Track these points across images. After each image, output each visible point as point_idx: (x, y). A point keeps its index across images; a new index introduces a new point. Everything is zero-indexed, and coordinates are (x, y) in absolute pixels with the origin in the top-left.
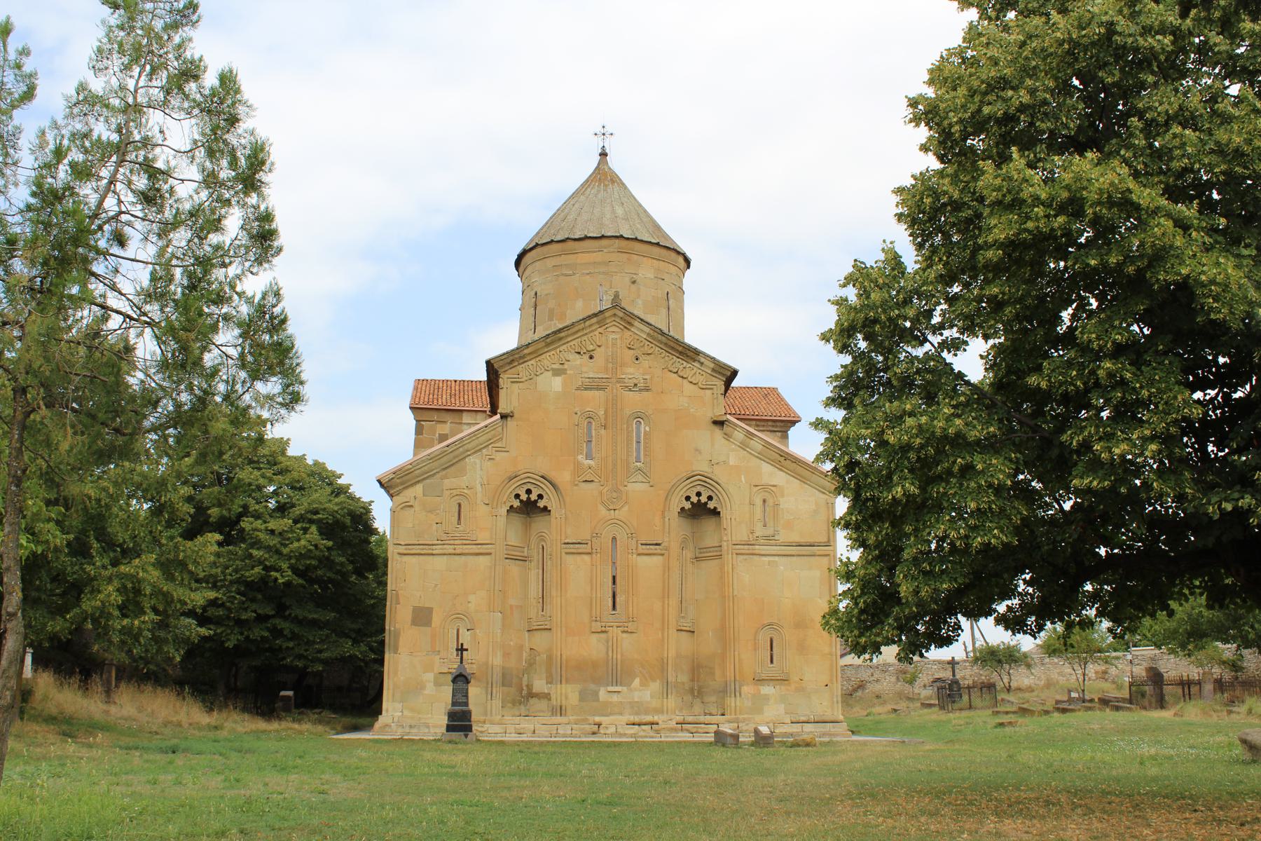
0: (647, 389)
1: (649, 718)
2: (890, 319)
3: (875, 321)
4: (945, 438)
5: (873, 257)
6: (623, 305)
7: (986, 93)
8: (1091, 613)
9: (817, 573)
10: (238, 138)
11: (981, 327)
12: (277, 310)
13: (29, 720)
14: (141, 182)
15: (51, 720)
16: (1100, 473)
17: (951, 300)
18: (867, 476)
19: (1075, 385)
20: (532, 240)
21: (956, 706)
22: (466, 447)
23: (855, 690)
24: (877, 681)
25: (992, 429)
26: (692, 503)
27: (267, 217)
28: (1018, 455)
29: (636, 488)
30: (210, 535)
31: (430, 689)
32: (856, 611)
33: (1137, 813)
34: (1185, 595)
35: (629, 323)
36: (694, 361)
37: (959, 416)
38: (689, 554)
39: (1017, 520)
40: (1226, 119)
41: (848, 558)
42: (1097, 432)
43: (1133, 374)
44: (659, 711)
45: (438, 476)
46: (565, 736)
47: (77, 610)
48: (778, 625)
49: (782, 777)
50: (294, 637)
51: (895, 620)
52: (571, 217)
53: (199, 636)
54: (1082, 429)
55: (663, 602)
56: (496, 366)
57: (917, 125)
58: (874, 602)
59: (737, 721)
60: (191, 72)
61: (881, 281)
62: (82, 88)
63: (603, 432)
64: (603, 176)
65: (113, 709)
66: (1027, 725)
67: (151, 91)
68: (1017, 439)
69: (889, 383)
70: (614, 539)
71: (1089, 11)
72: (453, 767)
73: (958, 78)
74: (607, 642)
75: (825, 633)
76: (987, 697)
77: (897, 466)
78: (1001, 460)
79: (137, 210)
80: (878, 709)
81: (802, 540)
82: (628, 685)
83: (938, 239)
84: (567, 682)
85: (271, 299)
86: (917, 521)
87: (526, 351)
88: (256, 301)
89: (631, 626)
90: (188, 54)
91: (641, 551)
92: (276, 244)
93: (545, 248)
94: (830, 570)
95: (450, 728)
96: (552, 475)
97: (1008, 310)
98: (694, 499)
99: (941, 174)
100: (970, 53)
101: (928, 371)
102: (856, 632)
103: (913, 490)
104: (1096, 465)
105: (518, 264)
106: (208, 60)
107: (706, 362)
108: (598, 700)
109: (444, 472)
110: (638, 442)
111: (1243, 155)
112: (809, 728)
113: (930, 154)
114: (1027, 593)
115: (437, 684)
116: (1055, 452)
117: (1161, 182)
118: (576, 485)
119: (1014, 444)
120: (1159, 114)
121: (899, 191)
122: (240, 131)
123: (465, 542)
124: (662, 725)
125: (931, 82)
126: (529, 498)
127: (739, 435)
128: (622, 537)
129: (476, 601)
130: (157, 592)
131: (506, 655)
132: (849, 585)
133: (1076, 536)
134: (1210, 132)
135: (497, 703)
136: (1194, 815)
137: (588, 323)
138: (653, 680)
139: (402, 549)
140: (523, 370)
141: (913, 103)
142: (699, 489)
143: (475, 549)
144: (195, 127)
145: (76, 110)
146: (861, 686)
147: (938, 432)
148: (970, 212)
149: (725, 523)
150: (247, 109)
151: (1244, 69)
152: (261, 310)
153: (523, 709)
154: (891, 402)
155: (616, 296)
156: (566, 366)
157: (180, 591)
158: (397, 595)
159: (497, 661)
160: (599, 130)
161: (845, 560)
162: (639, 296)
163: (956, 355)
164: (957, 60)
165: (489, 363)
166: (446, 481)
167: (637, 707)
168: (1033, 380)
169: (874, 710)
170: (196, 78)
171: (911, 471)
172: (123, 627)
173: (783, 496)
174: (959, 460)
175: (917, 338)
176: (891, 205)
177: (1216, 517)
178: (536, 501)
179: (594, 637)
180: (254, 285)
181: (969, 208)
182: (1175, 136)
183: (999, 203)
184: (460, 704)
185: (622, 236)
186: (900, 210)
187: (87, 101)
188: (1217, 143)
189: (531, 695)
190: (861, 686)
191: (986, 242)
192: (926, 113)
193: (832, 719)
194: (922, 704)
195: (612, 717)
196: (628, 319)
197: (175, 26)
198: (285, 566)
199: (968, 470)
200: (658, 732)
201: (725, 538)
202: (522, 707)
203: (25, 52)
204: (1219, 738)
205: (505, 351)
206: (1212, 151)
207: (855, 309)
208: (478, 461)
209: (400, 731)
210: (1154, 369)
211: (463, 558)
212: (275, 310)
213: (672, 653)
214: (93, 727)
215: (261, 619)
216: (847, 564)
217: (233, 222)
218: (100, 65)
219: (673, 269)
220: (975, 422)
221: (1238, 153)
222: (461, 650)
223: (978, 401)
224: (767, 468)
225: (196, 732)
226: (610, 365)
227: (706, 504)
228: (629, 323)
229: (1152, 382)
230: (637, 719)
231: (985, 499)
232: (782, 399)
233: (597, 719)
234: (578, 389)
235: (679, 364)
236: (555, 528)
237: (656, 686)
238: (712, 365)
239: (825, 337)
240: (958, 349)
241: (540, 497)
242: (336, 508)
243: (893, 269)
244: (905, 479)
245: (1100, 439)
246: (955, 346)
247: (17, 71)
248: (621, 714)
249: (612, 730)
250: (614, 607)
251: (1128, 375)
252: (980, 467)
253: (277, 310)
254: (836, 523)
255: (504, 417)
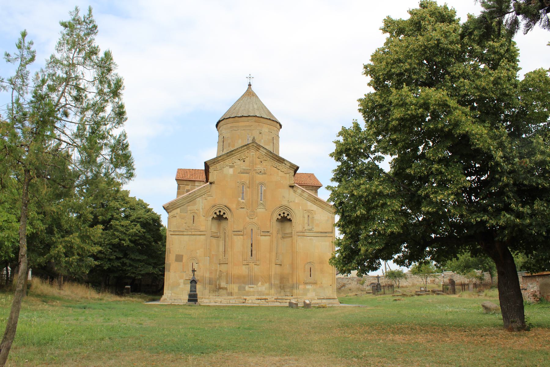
0: (265, 174)
1: (264, 297)
2: (355, 149)
3: (350, 149)
4: (375, 193)
5: (349, 126)
6: (256, 142)
7: (393, 64)
8: (428, 258)
9: (328, 243)
10: (111, 77)
11: (389, 150)
12: (125, 142)
13: (30, 296)
14: (74, 93)
15: (38, 296)
16: (432, 206)
17: (379, 142)
18: (346, 207)
19: (424, 173)
20: (222, 117)
21: (379, 293)
22: (196, 195)
23: (342, 287)
24: (350, 284)
25: (393, 190)
26: (281, 217)
27: (122, 107)
28: (403, 200)
29: (260, 210)
30: (99, 225)
31: (182, 286)
32: (342, 257)
33: (444, 332)
34: (463, 252)
35: (258, 149)
36: (283, 163)
37: (381, 185)
38: (280, 236)
39: (402, 224)
40: (479, 77)
41: (339, 238)
42: (432, 190)
43: (445, 170)
44: (268, 295)
45: (185, 205)
46: (232, 303)
47: (48, 254)
48: (313, 262)
49: (314, 319)
50: (130, 265)
51: (356, 261)
52: (237, 109)
53: (95, 265)
54: (426, 189)
55: (270, 254)
56: (208, 164)
57: (367, 75)
58: (349, 254)
59: (297, 298)
60: (94, 52)
61: (352, 134)
62: (52, 57)
63: (248, 189)
64: (249, 93)
65: (62, 292)
66: (405, 300)
67: (79, 58)
68: (402, 194)
69: (355, 173)
70: (252, 230)
71: (431, 35)
72: (190, 315)
73: (382, 59)
74: (249, 268)
75: (330, 266)
76: (391, 290)
77: (358, 204)
78: (397, 201)
79: (73, 103)
80: (350, 294)
81: (323, 231)
82: (257, 284)
83: (374, 119)
84: (234, 283)
85: (123, 138)
86: (366, 224)
87: (219, 159)
88: (117, 138)
89: (258, 263)
90: (93, 45)
91: (262, 234)
92: (125, 117)
93: (227, 120)
94: (332, 242)
95: (189, 300)
96: (229, 205)
97: (399, 144)
98: (282, 215)
99: (375, 94)
100: (386, 50)
101: (370, 169)
102: (342, 265)
103: (364, 212)
104: (431, 203)
105: (217, 126)
106: (100, 47)
107: (287, 164)
108: (245, 290)
109: (188, 204)
110: (261, 193)
111: (486, 89)
112: (324, 301)
113: (371, 87)
114: (405, 251)
115: (185, 284)
116: (416, 199)
117: (456, 99)
119: (401, 196)
120: (456, 73)
121: (360, 100)
122: (112, 74)
124: (269, 300)
125: (372, 60)
126: (220, 214)
127: (299, 191)
128: (255, 229)
129: (200, 253)
130: (79, 247)
131: (211, 273)
132: (339, 248)
133: (423, 230)
134: (473, 81)
135: (207, 291)
136: (465, 333)
137: (243, 148)
138: (266, 283)
139: (172, 233)
140: (218, 165)
141: (366, 67)
142: (284, 211)
143: (199, 233)
144: (95, 72)
145: (50, 65)
146: (344, 285)
147: (373, 191)
148: (386, 108)
149: (294, 224)
150: (115, 66)
151: (486, 59)
152: (119, 142)
153: (217, 294)
154: (356, 180)
155: (254, 138)
156: (234, 165)
157: (88, 246)
158: (170, 250)
159: (207, 275)
160: (248, 76)
161: (338, 238)
162: (262, 139)
163: (380, 162)
164: (382, 52)
165: (205, 163)
166: (189, 207)
167: (260, 293)
168: (408, 171)
169: (348, 295)
170: (96, 54)
171: (363, 205)
172: (66, 261)
173: (315, 214)
174: (381, 201)
175: (365, 156)
176: (357, 106)
177: (474, 223)
178: (223, 215)
179: (244, 267)
180: (116, 132)
181: (386, 107)
182: (461, 82)
183: (397, 105)
184: (193, 291)
185: (256, 116)
186: (360, 108)
187: (54, 62)
188: (476, 85)
189: (220, 288)
190: (344, 285)
191: (392, 119)
192: (370, 71)
193: (332, 297)
194: (367, 292)
195: (250, 297)
196: (258, 147)
197: (88, 34)
198: (127, 239)
199: (384, 205)
200: (267, 302)
201: (293, 230)
202: (217, 293)
203: (31, 43)
204: (475, 305)
205: (211, 158)
206: (474, 88)
207: (342, 144)
208: (201, 200)
209: (170, 301)
210: (453, 168)
211: (195, 236)
212: (124, 142)
213: (273, 273)
214: (54, 299)
215: (118, 258)
216: (339, 239)
217: (109, 108)
218: (59, 49)
219: (275, 129)
220: (387, 187)
221: (484, 89)
222: (194, 271)
223: (388, 180)
224: (309, 204)
225: (93, 301)
226: (251, 164)
227: (286, 217)
228: (258, 149)
229: (452, 173)
230: (260, 297)
231: (391, 215)
232: (316, 178)
233: (245, 297)
234: (239, 173)
235: (277, 164)
236: (229, 226)
237: (267, 285)
238: (289, 165)
239: (331, 155)
240: (381, 160)
241: (224, 213)
242: (147, 217)
243: (356, 130)
244: (361, 208)
245: (433, 193)
246: (380, 159)
247: (28, 50)
248: (254, 296)
249: (250, 301)
250: (252, 255)
251: (443, 170)
252: (389, 203)
253: (125, 142)
254: (335, 225)
255: (211, 183)
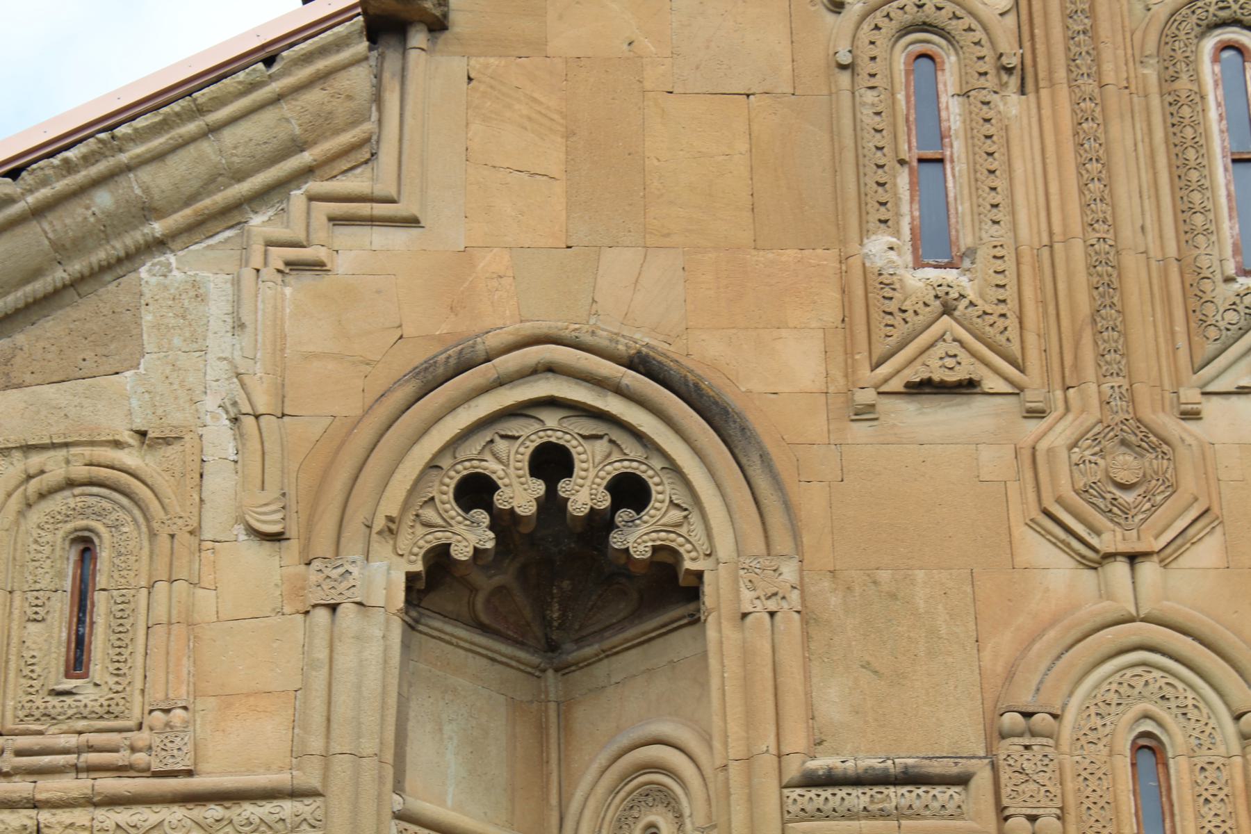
22: (134, 185)
63: (1012, 105)
118: (864, 413)
123: (110, 784)
126: (552, 504)
178: (600, 523)
208: (217, 286)
